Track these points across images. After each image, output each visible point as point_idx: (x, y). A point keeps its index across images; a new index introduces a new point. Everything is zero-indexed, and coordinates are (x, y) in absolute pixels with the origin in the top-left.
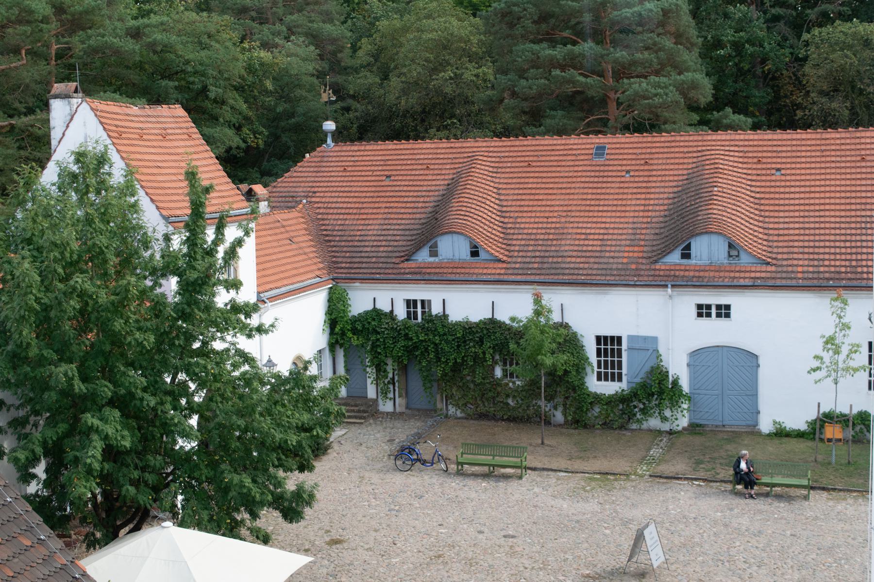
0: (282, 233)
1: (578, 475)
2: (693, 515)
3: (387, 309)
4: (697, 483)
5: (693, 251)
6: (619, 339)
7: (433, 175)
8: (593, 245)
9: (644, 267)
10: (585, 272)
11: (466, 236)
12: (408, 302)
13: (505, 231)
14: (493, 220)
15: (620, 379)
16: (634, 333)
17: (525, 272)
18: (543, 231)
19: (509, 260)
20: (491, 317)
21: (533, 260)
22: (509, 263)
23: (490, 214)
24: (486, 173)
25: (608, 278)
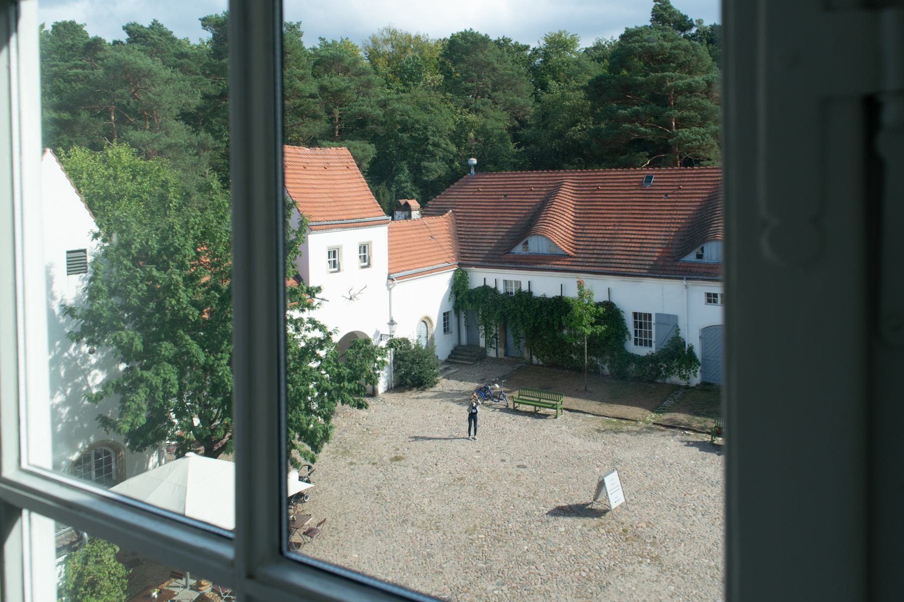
0: (425, 232)
1: (600, 418)
2: (671, 461)
3: (493, 286)
4: (687, 432)
5: (705, 255)
6: (650, 315)
7: (534, 195)
8: (634, 247)
9: (668, 264)
10: (626, 266)
11: (546, 237)
12: (505, 282)
13: (576, 234)
14: (568, 227)
15: (651, 345)
16: (660, 312)
17: (585, 264)
18: (602, 236)
19: (575, 255)
20: (560, 295)
21: (592, 256)
22: (575, 257)
23: (566, 222)
24: (569, 194)
25: (642, 271)
